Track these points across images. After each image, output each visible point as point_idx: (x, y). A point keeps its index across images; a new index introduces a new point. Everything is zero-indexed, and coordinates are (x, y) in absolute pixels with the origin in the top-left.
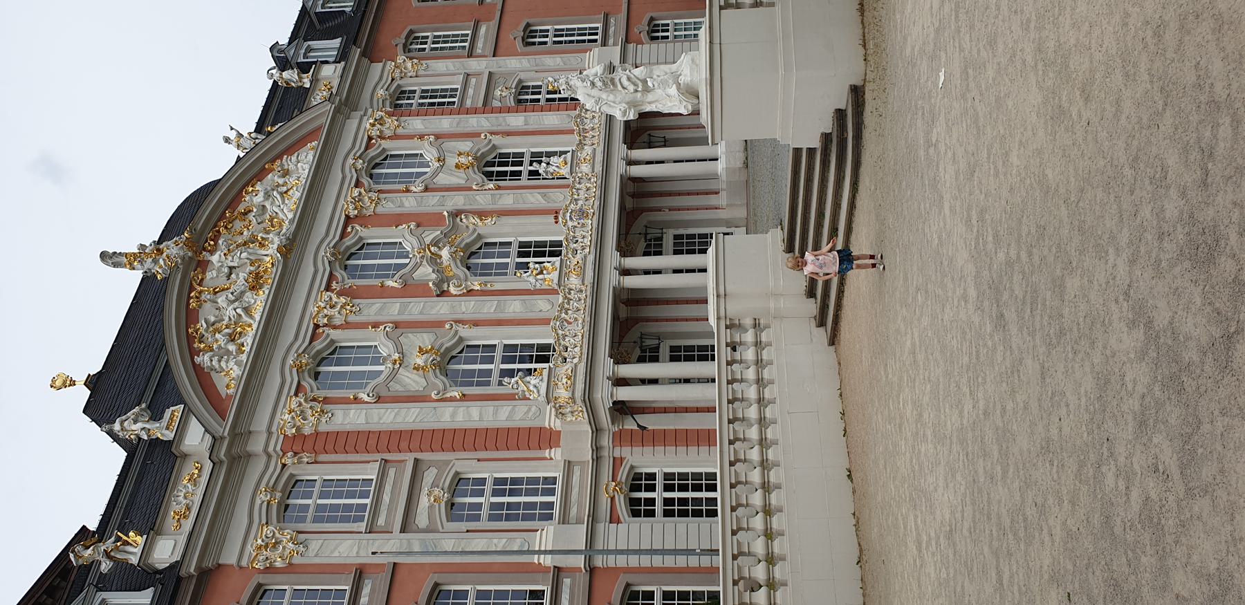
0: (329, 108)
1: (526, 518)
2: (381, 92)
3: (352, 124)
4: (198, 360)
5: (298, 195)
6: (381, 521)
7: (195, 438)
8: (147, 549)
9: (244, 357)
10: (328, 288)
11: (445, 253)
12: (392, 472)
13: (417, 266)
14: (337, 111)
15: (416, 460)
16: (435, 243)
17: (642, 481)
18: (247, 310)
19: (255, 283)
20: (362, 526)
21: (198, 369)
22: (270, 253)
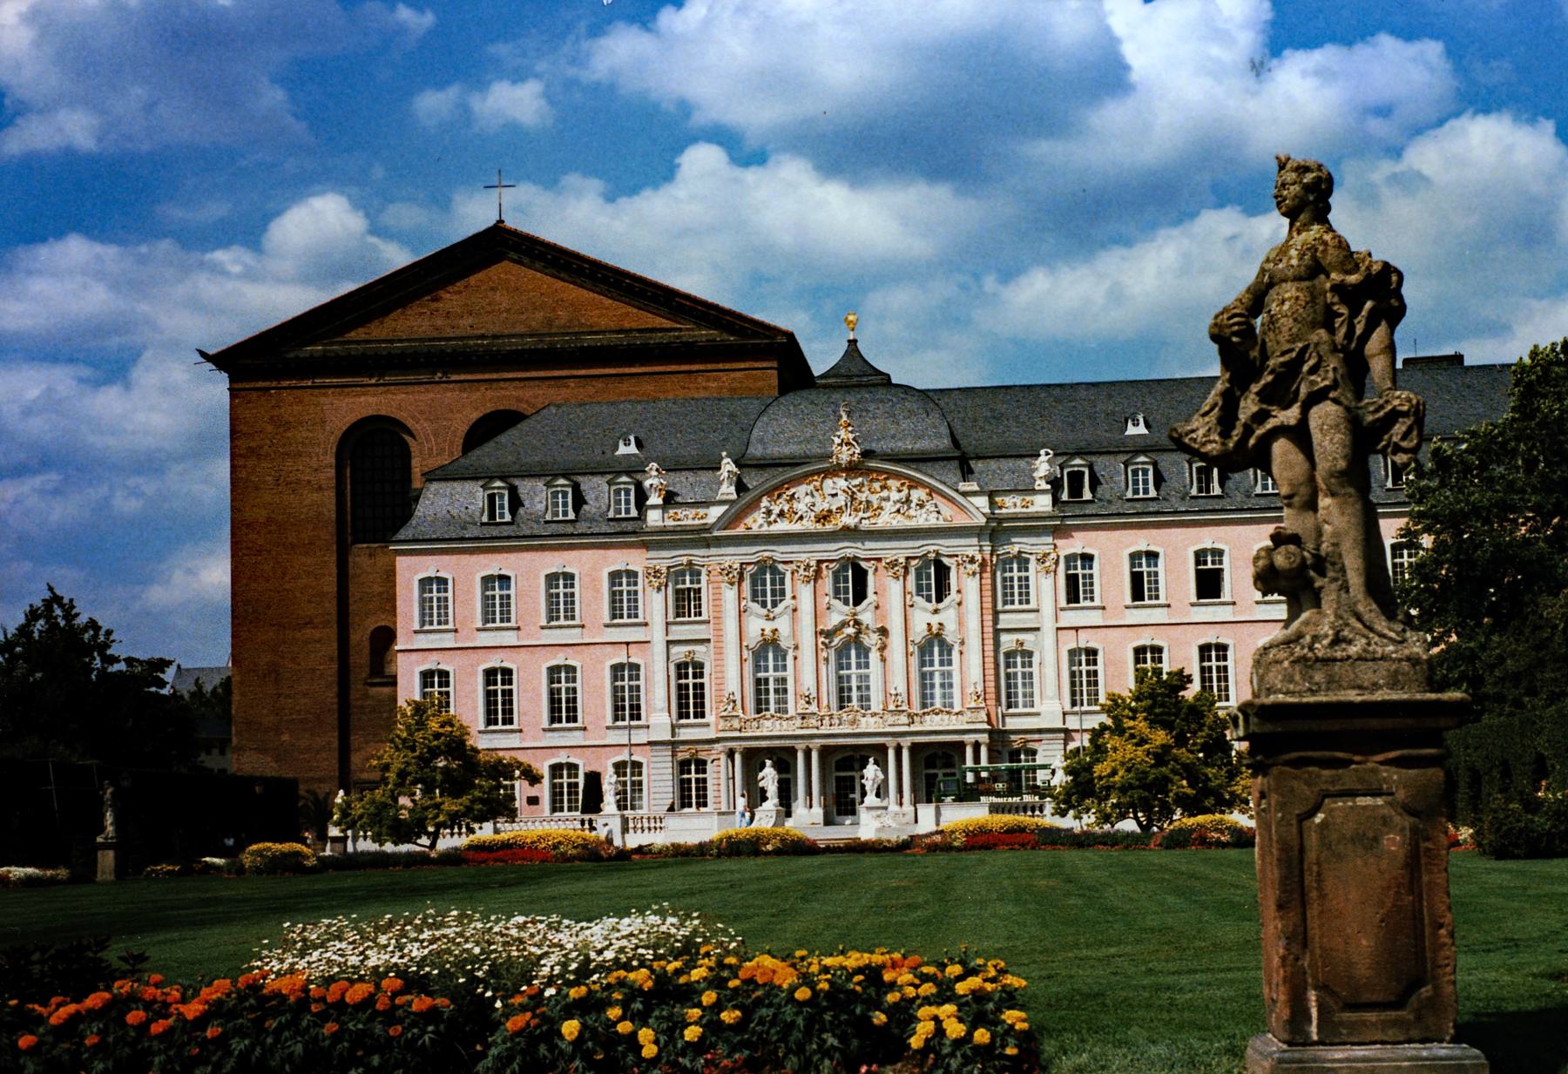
0: (983, 521)
1: (680, 706)
2: (1016, 549)
3: (974, 541)
4: (765, 499)
5: (894, 523)
6: (673, 628)
7: (715, 513)
8: (654, 507)
9: (765, 528)
10: (819, 562)
11: (850, 631)
12: (703, 627)
13: (840, 613)
14: (981, 528)
15: (708, 641)
16: (857, 623)
17: (701, 766)
18: (801, 518)
19: (824, 517)
20: (671, 619)
21: (759, 499)
22: (848, 520)
